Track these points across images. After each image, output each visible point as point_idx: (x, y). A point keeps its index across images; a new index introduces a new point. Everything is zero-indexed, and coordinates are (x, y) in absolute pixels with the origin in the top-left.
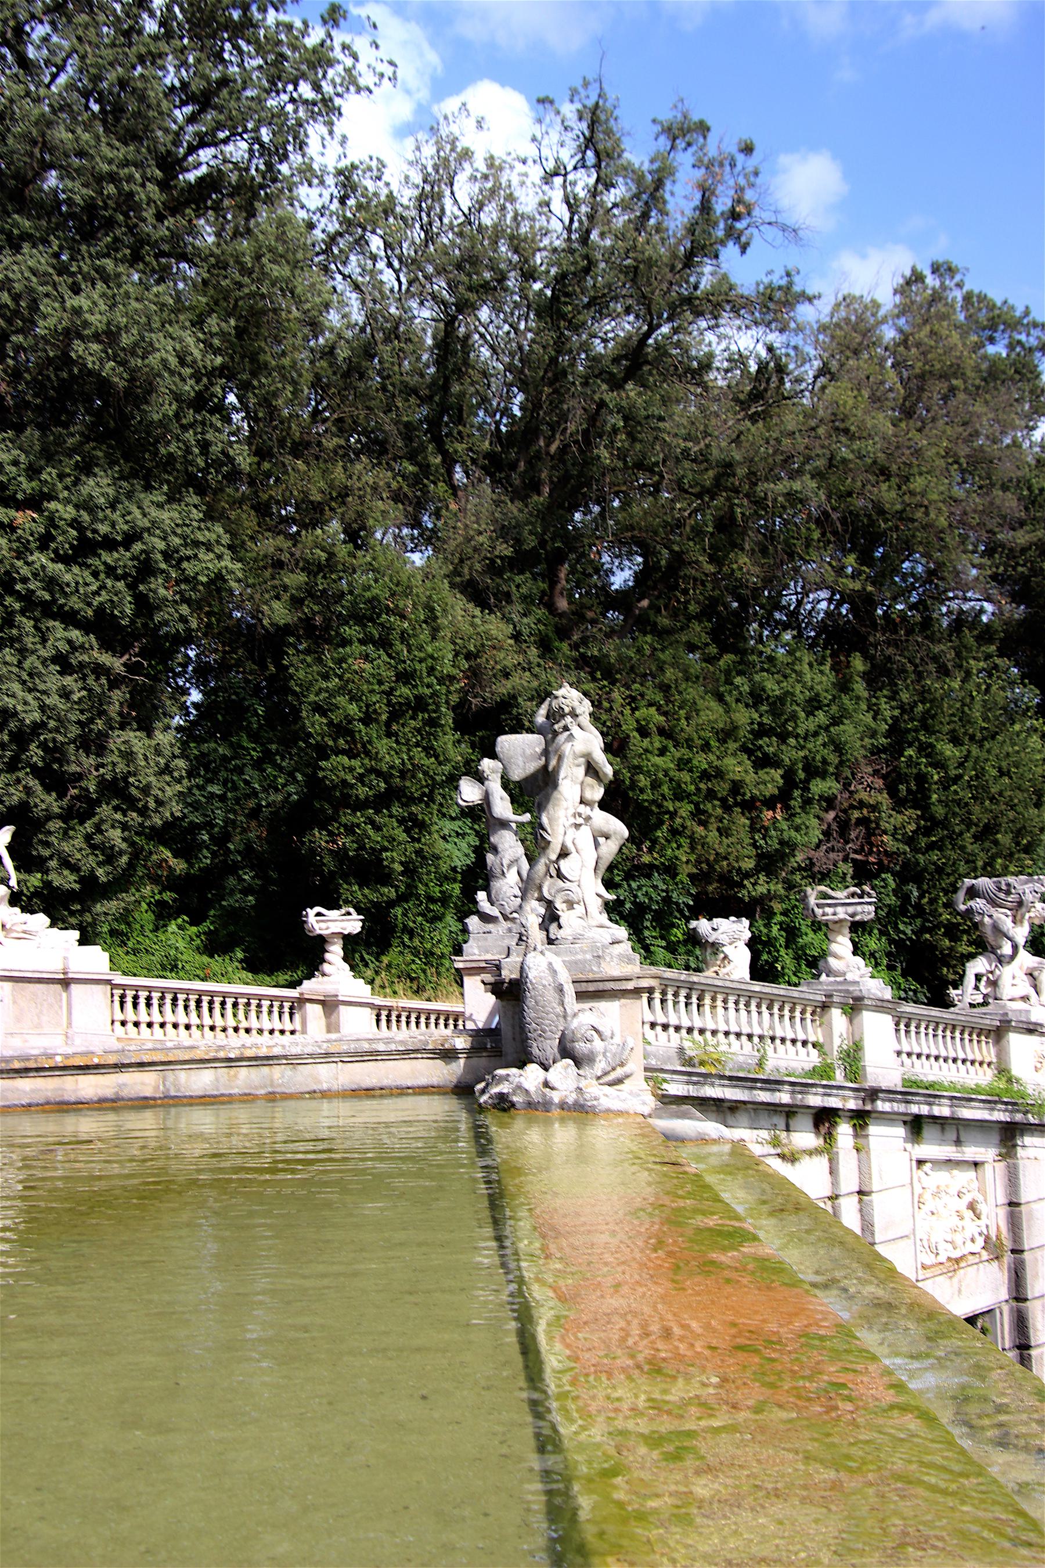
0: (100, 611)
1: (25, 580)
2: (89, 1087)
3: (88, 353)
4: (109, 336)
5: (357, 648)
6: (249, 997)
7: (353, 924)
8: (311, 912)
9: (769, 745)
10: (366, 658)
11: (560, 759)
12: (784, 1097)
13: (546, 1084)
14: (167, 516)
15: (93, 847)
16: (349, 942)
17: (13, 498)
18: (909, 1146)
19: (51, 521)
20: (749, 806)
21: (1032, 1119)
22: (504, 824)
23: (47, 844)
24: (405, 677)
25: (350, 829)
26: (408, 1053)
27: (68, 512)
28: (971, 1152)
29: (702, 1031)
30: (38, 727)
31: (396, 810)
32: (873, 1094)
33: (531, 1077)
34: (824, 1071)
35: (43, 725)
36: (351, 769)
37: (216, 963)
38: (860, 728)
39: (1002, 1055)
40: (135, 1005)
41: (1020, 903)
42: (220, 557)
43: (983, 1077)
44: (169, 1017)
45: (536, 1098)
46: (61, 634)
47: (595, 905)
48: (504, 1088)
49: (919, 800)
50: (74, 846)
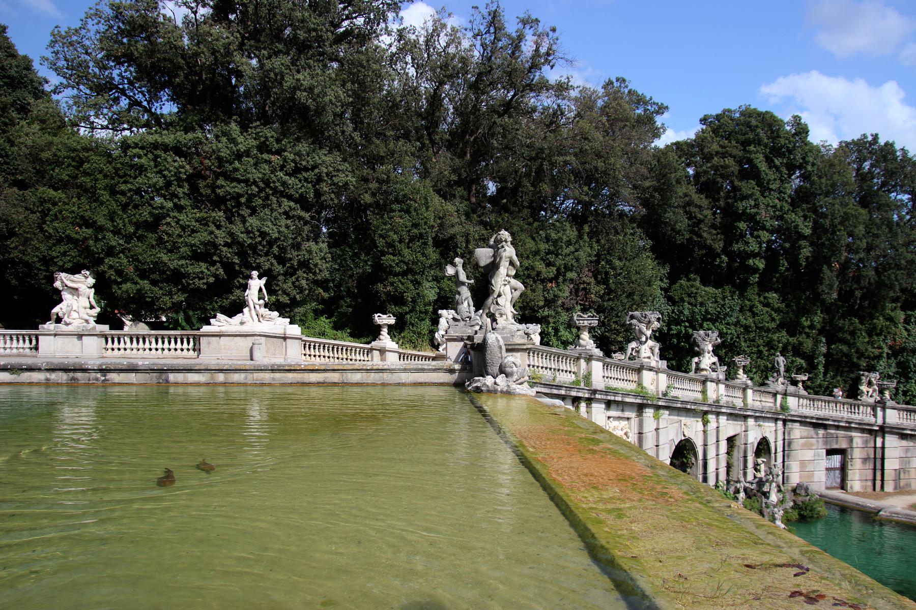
0: (301, 195)
1: (274, 182)
2: (314, 377)
3: (302, 96)
4: (310, 90)
5: (397, 213)
6: (352, 347)
7: (392, 321)
8: (376, 315)
9: (551, 258)
10: (401, 217)
11: (501, 258)
12: (563, 392)
13: (495, 383)
14: (328, 159)
15: (295, 287)
16: (390, 327)
17: (271, 150)
19: (285, 160)
20: (543, 281)
21: (649, 402)
22: (463, 284)
23: (277, 285)
24: (415, 225)
25: (392, 284)
26: (435, 370)
27: (292, 156)
28: (627, 414)
29: (533, 366)
30: (277, 239)
31: (410, 277)
32: (595, 392)
33: (489, 380)
34: (577, 382)
35: (279, 239)
36: (394, 261)
37: (339, 333)
38: (585, 254)
39: (640, 378)
40: (309, 348)
41: (649, 322)
42: (347, 176)
43: (632, 386)
44: (322, 353)
45: (491, 389)
46: (286, 204)
47: (510, 316)
48: (478, 384)
49: (605, 282)
50: (288, 286)
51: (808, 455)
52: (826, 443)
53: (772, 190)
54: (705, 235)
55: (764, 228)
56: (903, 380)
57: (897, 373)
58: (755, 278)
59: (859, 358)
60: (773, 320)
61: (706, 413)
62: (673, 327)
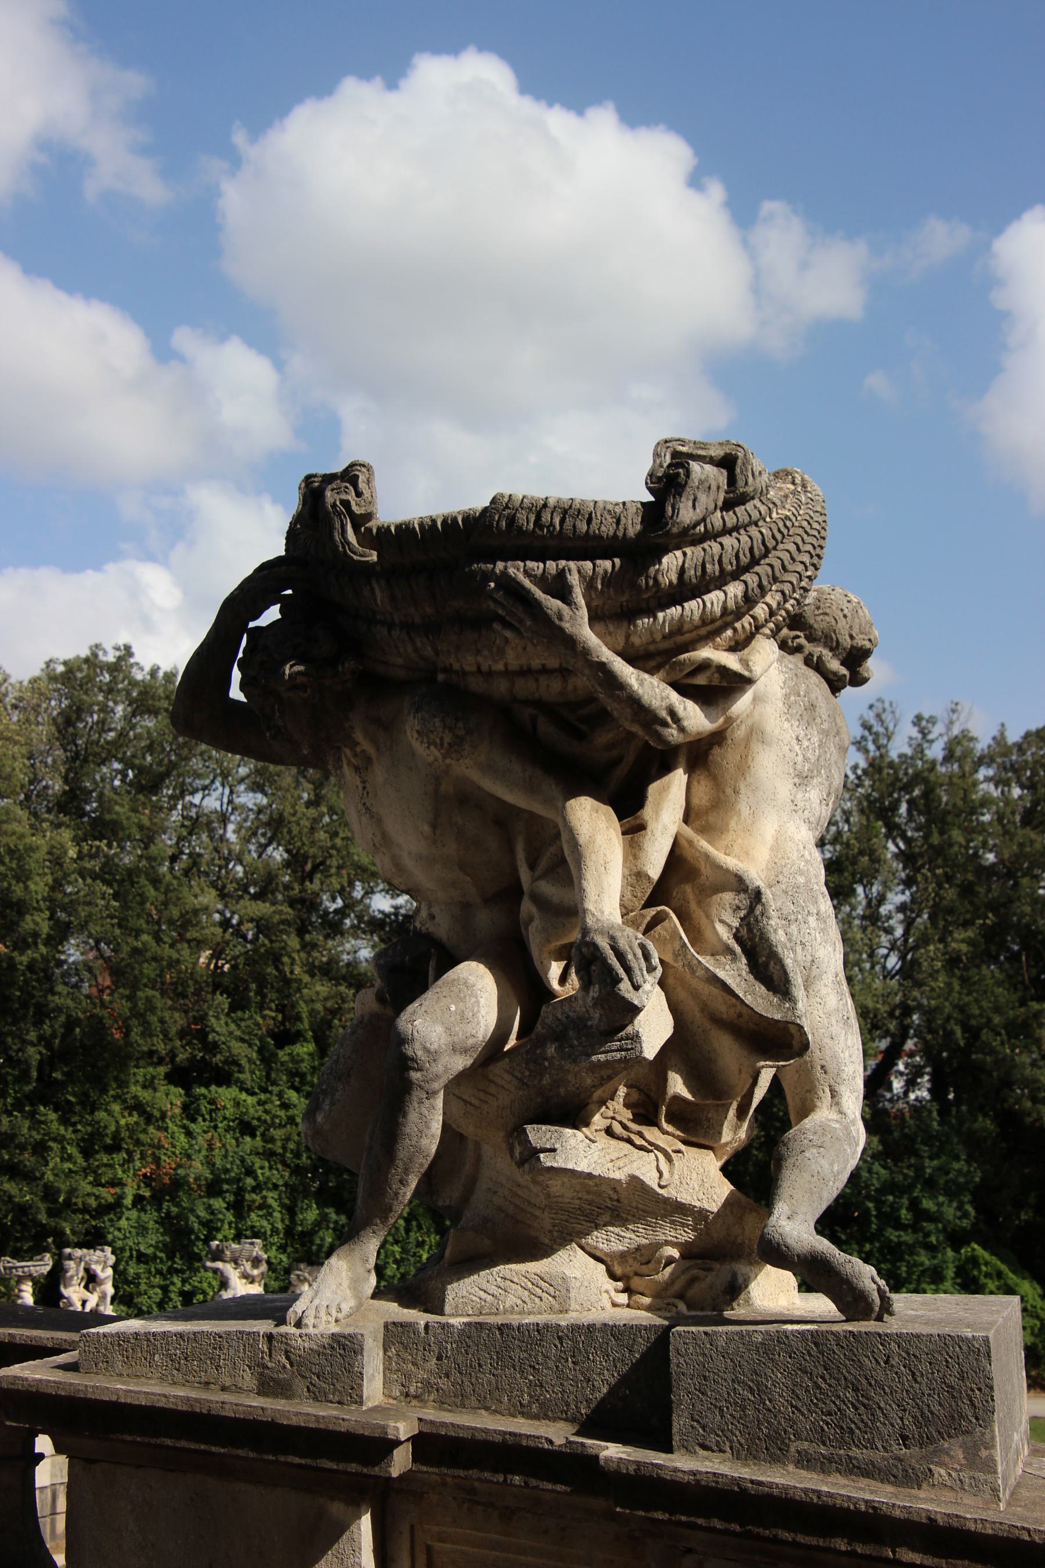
56: (179, 1263)
57: (165, 1248)
59: (51, 1213)
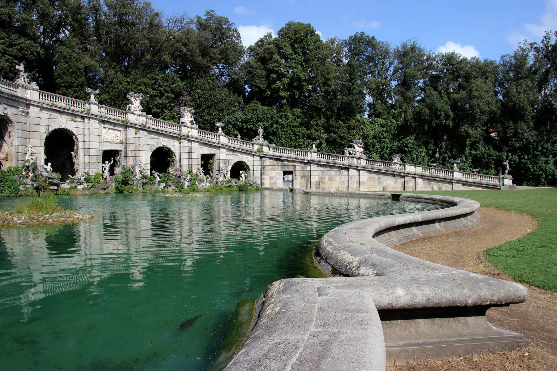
9: (155, 86)
18: (102, 125)
25: (62, 90)
28: (117, 128)
51: (274, 173)
52: (283, 168)
53: (291, 59)
54: (257, 81)
55: (284, 76)
58: (285, 101)
60: (296, 122)
61: (181, 139)
62: (244, 124)
